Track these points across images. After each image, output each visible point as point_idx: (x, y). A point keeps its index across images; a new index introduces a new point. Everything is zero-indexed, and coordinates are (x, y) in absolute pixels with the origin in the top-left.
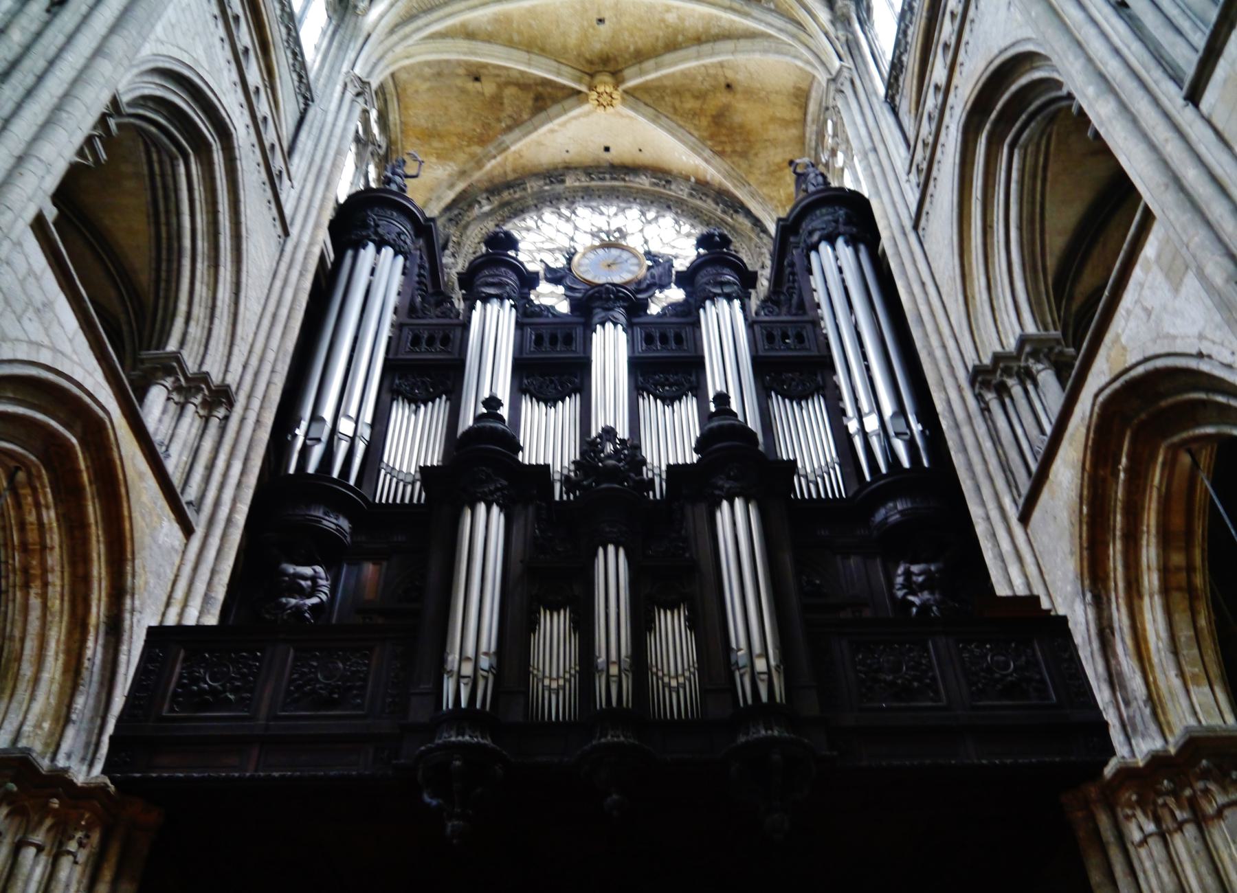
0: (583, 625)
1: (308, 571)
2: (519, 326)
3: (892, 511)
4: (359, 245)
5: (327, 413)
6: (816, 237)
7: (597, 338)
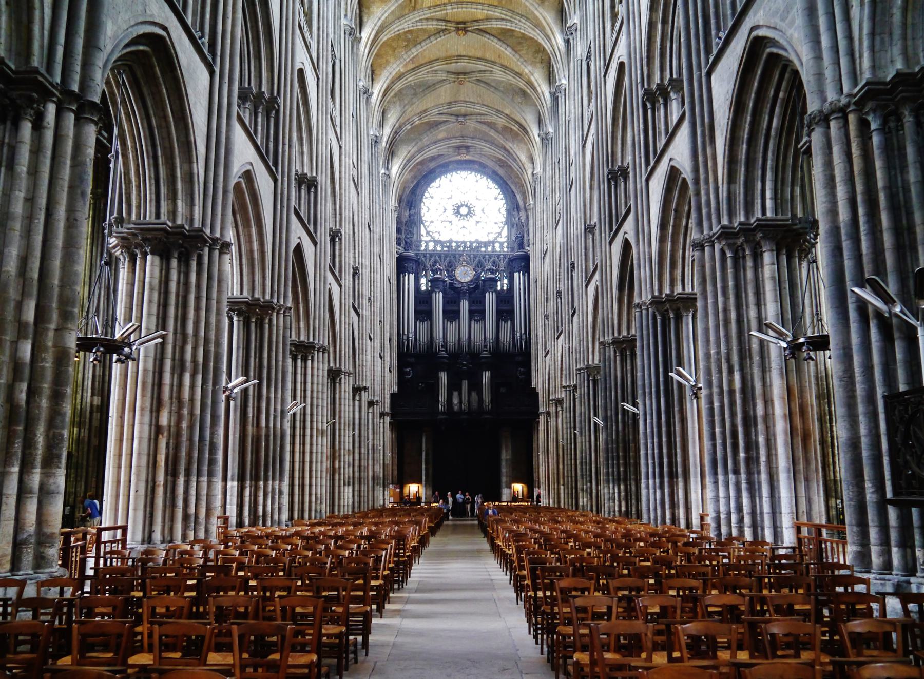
0: (460, 394)
1: (408, 370)
2: (444, 297)
3: (520, 359)
4: (404, 273)
5: (406, 333)
6: (516, 269)
7: (462, 303)
